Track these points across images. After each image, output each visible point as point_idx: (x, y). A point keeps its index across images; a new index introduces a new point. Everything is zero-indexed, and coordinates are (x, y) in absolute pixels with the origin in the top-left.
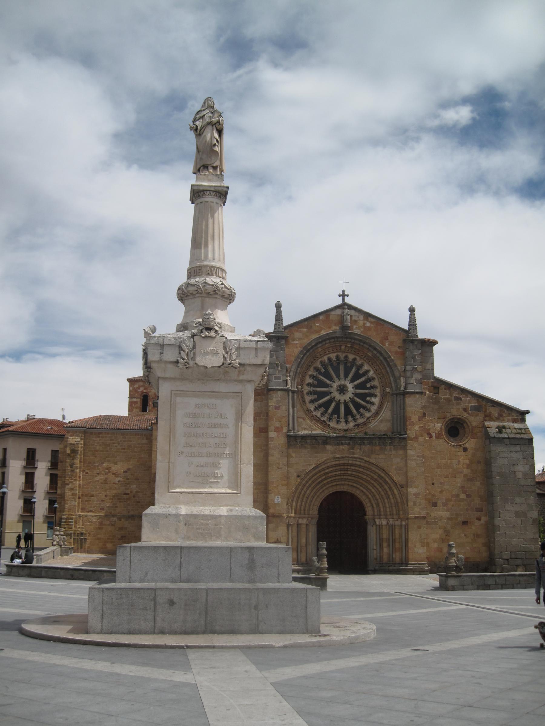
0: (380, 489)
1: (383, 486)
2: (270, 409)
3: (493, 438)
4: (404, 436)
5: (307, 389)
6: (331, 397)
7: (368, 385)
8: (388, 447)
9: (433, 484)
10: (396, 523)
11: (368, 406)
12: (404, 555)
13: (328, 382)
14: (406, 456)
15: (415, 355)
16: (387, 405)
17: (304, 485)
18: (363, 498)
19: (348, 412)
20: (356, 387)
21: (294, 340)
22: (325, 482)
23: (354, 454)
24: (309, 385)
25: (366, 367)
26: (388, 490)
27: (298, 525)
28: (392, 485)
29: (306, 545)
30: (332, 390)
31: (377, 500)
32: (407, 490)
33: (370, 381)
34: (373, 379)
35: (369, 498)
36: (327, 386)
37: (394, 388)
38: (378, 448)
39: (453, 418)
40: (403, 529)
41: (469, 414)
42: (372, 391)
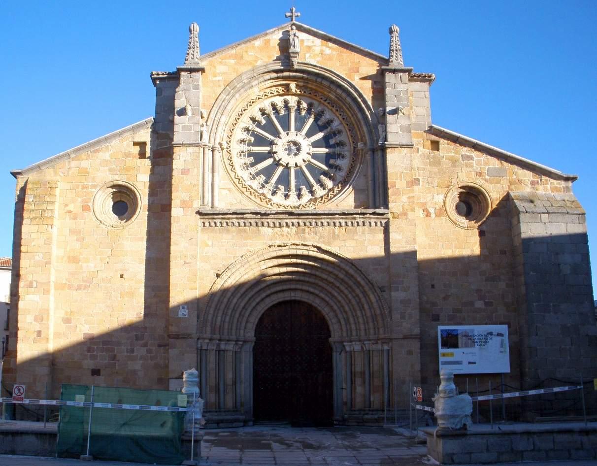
0: (350, 296)
1: (354, 291)
2: (174, 173)
8: (360, 228)
9: (433, 286)
10: (374, 347)
12: (386, 397)
15: (399, 92)
18: (325, 311)
21: (215, 76)
23: (305, 239)
26: (361, 295)
27: (219, 351)
28: (367, 288)
29: (235, 383)
31: (346, 313)
33: (335, 135)
34: (340, 132)
35: (335, 311)
37: (368, 142)
41: (486, 180)
42: (338, 150)
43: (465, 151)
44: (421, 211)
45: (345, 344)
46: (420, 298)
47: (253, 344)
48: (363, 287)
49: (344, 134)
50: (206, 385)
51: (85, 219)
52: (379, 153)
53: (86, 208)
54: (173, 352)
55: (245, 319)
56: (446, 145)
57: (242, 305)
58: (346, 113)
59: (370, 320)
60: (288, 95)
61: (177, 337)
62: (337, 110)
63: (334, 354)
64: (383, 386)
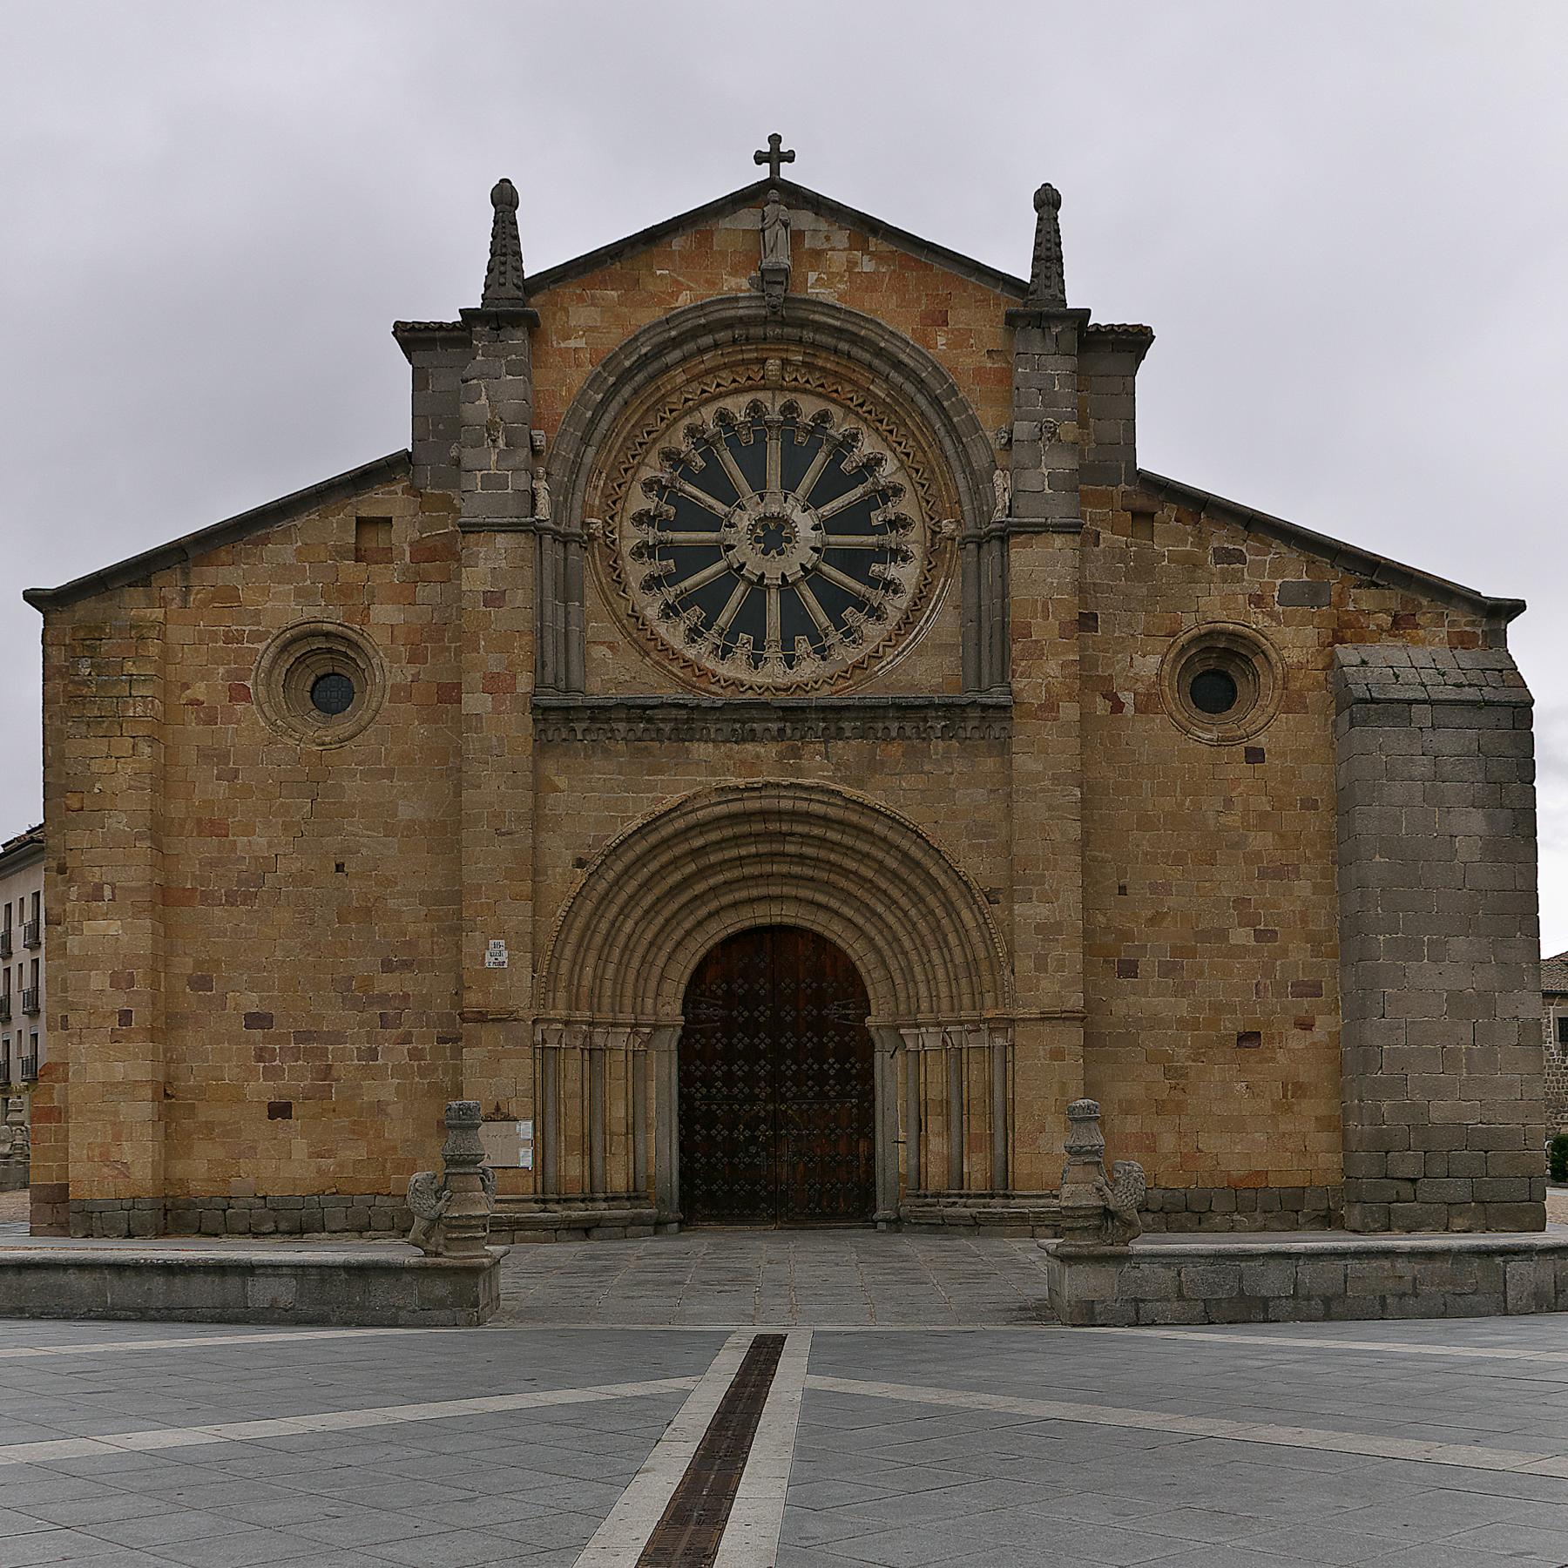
0: (913, 912)
3: (1365, 701)
4: (1003, 700)
5: (632, 536)
6: (730, 566)
7: (877, 518)
9: (1123, 890)
10: (973, 1041)
11: (876, 596)
13: (720, 508)
14: (1009, 781)
16: (947, 589)
17: (605, 898)
18: (855, 949)
19: (796, 621)
20: (830, 525)
22: (700, 888)
24: (641, 518)
25: (868, 446)
26: (940, 912)
28: (954, 894)
29: (631, 1129)
30: (730, 536)
31: (905, 953)
32: (1011, 910)
33: (886, 500)
34: (897, 491)
35: (878, 951)
36: (714, 523)
37: (969, 516)
38: (895, 749)
39: (1210, 634)
40: (998, 1061)
41: (1272, 615)
42: (892, 539)
43: (1221, 538)
44: (1099, 699)
45: (902, 1031)
46: (1086, 920)
47: (679, 1031)
48: (944, 891)
49: (908, 495)
50: (558, 1134)
51: (238, 722)
52: (995, 544)
53: (239, 693)
54: (472, 1056)
55: (656, 971)
56: (1173, 523)
57: (649, 936)
58: (916, 440)
59: (962, 974)
60: (764, 388)
61: (481, 1018)
62: (891, 432)
63: (878, 1056)
64: (992, 1135)
